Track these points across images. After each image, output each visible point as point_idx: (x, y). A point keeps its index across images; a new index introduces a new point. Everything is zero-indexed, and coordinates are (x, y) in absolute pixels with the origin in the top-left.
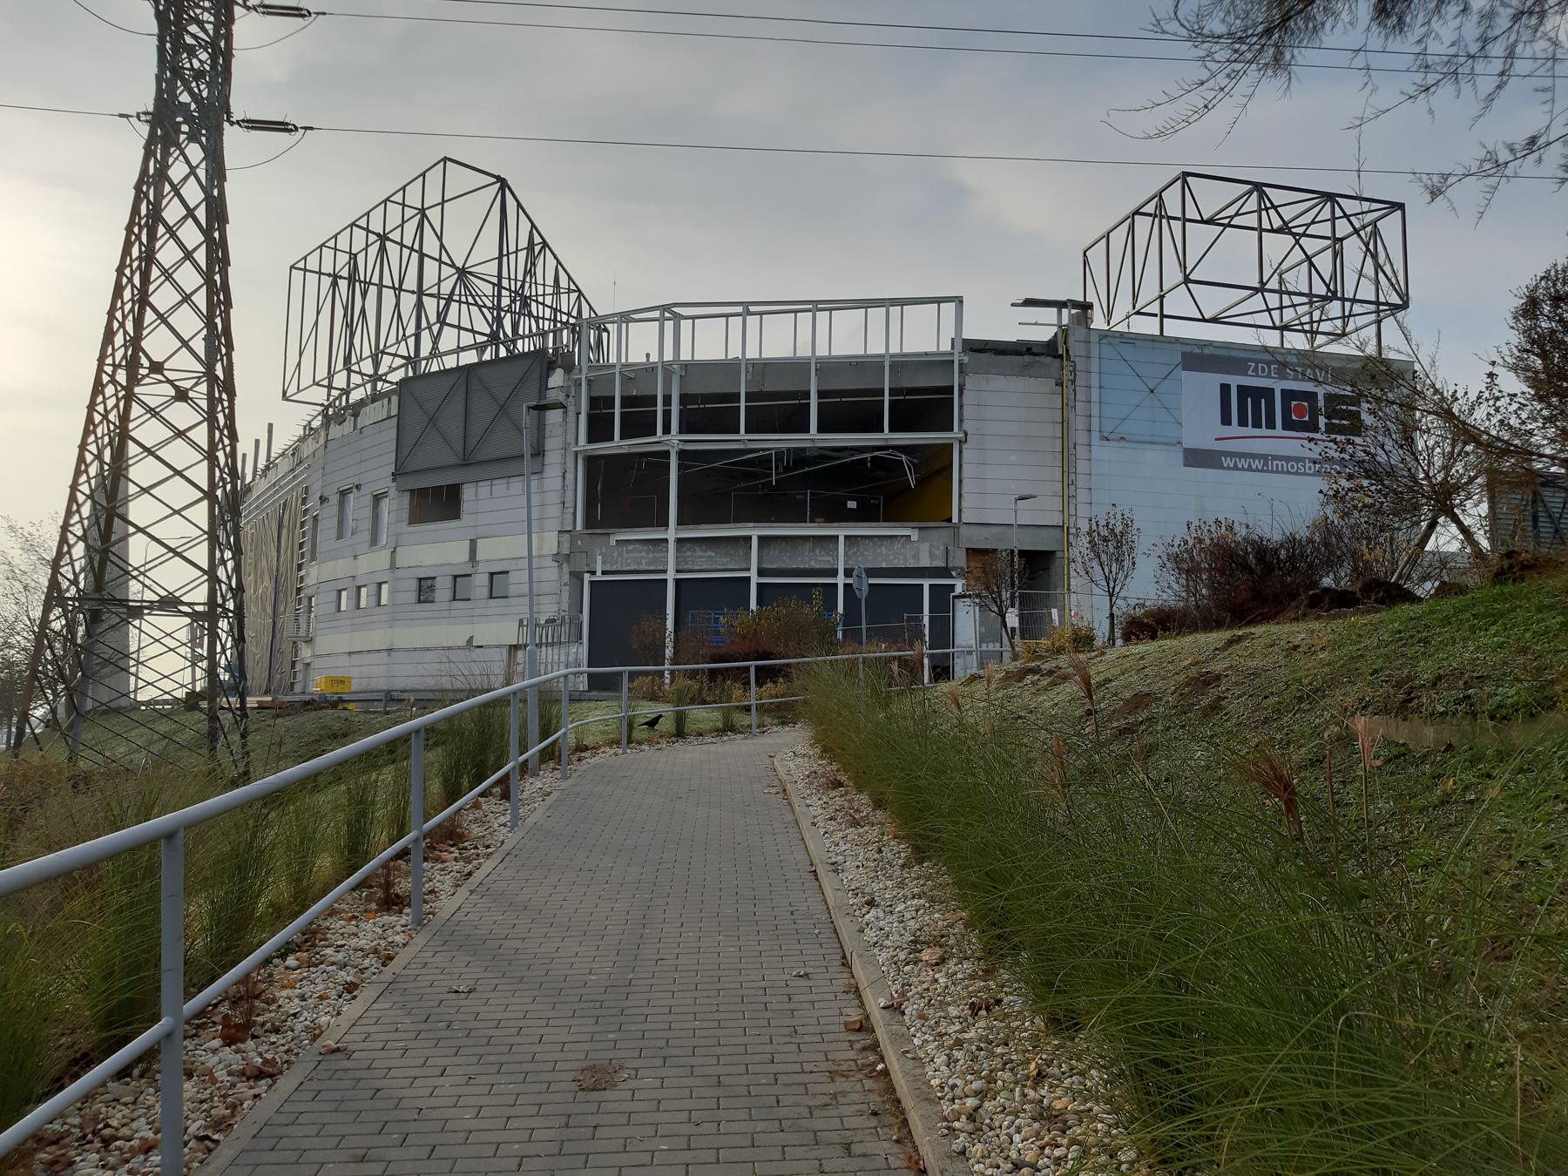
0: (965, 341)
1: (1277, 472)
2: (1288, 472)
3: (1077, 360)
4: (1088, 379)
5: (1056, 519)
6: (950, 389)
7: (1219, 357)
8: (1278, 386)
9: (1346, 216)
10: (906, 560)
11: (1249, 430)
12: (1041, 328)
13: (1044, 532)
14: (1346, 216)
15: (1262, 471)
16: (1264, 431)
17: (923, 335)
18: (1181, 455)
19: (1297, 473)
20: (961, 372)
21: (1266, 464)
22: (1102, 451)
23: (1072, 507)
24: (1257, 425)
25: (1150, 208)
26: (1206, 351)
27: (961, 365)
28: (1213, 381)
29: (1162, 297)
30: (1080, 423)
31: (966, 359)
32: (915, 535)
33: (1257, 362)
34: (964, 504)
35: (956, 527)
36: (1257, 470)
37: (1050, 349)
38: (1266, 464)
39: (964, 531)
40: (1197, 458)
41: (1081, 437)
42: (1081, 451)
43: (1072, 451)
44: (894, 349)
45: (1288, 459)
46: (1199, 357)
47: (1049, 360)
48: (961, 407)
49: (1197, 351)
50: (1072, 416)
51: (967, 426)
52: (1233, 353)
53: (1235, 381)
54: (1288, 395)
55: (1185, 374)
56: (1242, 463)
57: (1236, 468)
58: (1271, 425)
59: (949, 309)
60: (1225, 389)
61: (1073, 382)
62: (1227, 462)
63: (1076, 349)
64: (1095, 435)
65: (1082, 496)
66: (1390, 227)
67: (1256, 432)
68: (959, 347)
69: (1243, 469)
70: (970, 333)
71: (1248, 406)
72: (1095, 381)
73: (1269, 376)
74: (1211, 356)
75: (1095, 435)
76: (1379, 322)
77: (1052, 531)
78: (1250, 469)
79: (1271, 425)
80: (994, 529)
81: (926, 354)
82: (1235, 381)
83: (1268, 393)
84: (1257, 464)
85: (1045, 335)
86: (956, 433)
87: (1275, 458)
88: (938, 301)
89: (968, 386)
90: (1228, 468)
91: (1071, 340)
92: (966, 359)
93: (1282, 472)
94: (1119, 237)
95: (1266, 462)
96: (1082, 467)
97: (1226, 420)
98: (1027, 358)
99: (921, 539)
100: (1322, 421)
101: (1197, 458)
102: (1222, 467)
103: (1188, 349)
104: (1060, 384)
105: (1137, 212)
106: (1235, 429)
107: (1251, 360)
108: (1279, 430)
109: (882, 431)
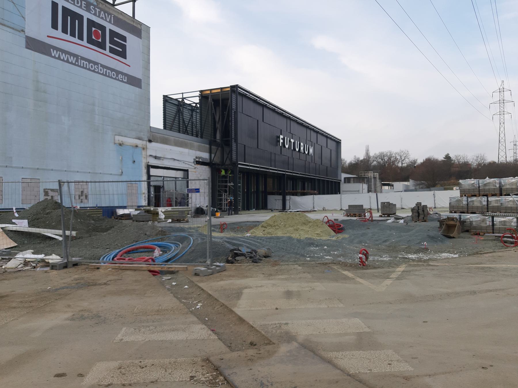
1: (83, 67)
2: (89, 69)
8: (86, 15)
11: (68, 37)
15: (75, 64)
16: (76, 40)
19: (94, 71)
24: (73, 35)
36: (71, 63)
40: (33, 44)
45: (90, 61)
54: (91, 23)
57: (59, 58)
58: (81, 38)
62: (54, 53)
67: (72, 39)
69: (63, 60)
73: (81, 7)
78: (67, 61)
79: (81, 38)
84: (71, 59)
87: (83, 58)
90: (54, 57)
93: (86, 68)
95: (77, 60)
97: (55, 26)
100: (108, 45)
101: (33, 44)
106: (59, 33)
108: (85, 42)
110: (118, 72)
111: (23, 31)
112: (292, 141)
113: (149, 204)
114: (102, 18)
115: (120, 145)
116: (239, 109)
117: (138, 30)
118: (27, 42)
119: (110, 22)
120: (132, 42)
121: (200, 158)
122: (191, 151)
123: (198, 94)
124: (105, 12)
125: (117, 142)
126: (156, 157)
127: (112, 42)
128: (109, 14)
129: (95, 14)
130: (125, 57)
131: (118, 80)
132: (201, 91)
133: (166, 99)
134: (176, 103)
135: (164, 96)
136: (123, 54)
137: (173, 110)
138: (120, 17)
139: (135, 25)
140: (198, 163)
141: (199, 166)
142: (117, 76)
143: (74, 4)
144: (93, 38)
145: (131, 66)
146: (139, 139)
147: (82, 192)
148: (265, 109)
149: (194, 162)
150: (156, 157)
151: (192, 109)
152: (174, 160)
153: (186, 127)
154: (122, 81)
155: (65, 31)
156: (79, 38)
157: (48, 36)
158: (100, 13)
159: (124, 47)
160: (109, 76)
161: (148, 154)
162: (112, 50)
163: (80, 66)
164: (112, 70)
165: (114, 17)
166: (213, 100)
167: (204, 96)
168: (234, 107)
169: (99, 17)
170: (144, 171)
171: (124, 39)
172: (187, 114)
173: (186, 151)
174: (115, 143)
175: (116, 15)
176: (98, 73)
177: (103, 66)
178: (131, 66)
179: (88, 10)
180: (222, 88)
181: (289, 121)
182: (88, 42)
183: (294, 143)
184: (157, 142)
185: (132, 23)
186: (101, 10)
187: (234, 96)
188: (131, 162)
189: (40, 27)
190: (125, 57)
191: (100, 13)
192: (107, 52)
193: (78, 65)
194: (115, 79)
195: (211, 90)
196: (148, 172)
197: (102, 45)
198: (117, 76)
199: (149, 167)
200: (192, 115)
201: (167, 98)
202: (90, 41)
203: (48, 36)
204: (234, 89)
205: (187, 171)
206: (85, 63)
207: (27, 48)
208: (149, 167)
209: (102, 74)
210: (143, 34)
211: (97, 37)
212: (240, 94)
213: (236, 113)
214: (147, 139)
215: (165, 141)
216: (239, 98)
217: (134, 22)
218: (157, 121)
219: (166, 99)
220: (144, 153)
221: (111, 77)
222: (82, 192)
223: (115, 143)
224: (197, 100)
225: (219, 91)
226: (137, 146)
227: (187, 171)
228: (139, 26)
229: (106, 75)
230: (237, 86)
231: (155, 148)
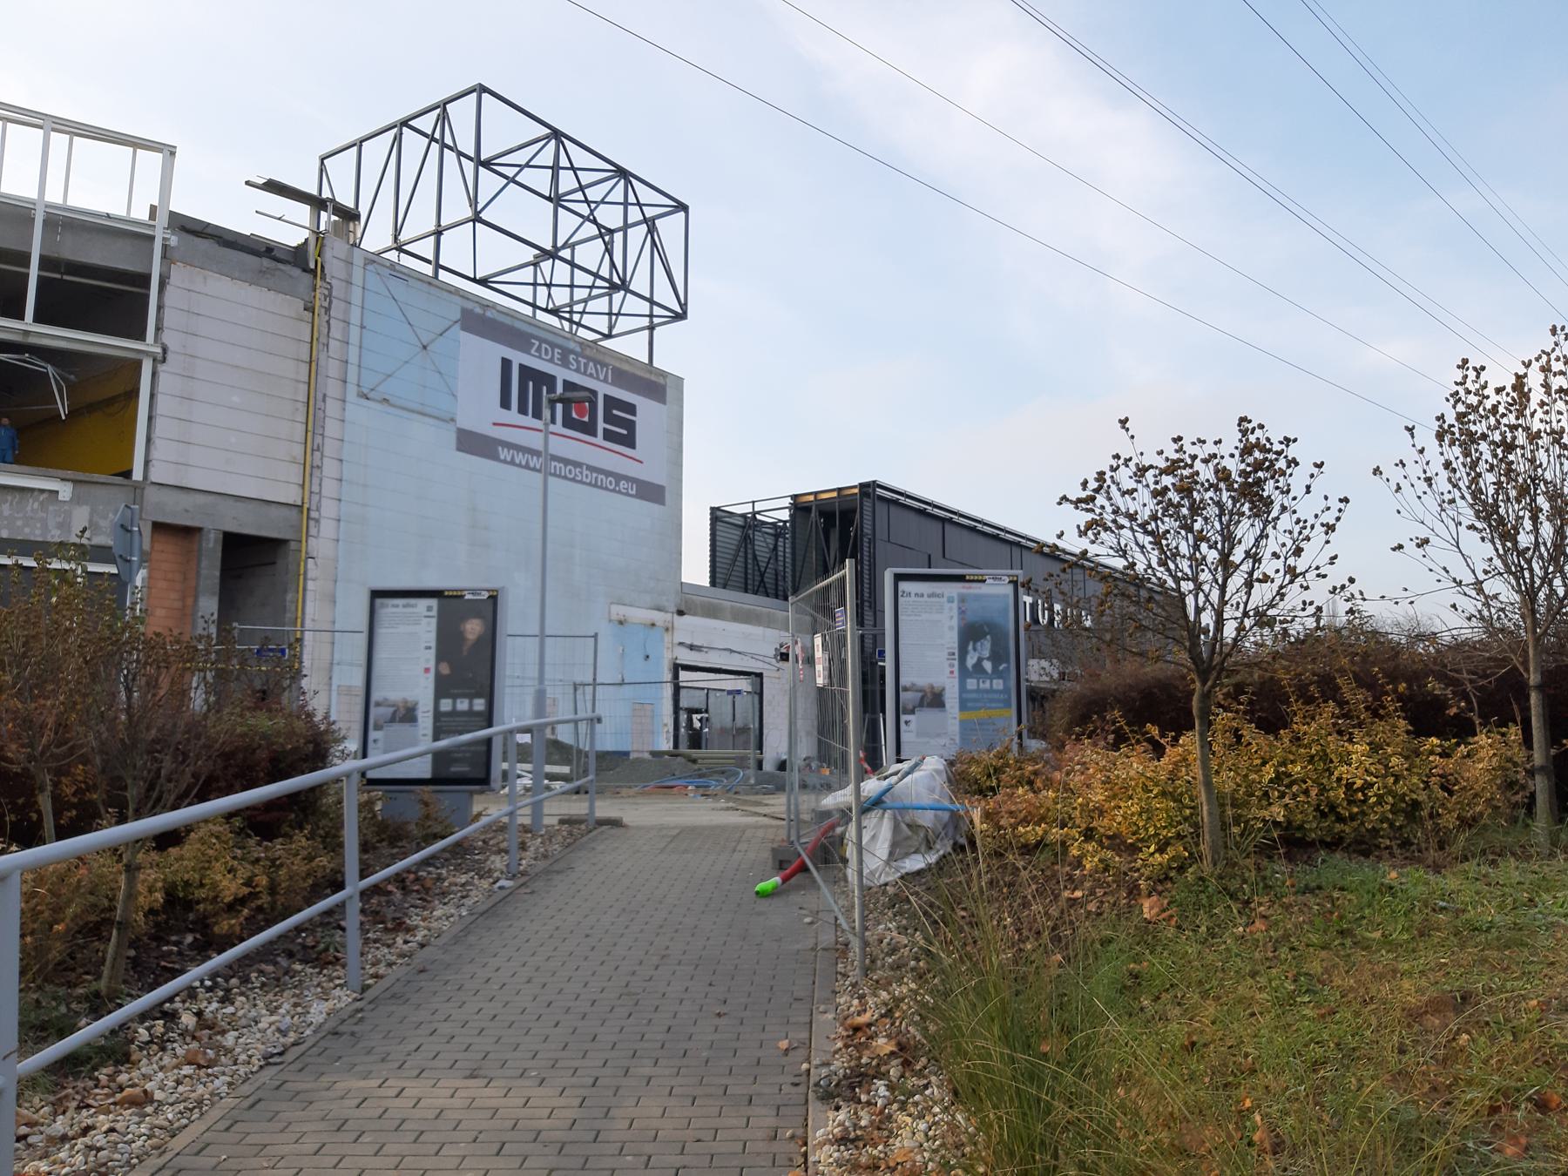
0: (173, 215)
2: (565, 477)
3: (334, 282)
4: (347, 312)
5: (291, 495)
6: (144, 280)
7: (502, 324)
8: (562, 374)
9: (638, 204)
10: (45, 528)
11: (529, 420)
12: (288, 226)
13: (274, 511)
14: (638, 204)
17: (103, 187)
18: (452, 438)
19: (573, 480)
20: (164, 257)
22: (358, 411)
23: (316, 481)
25: (427, 123)
26: (488, 314)
27: (165, 247)
28: (497, 351)
29: (438, 233)
30: (332, 368)
31: (174, 241)
32: (65, 491)
34: (155, 454)
35: (138, 488)
37: (297, 256)
39: (151, 494)
40: (473, 443)
41: (333, 389)
42: (332, 408)
43: (320, 404)
44: (54, 196)
45: (566, 462)
46: (482, 322)
47: (297, 272)
48: (160, 308)
49: (478, 310)
50: (323, 356)
51: (167, 337)
52: (518, 325)
53: (518, 358)
55: (466, 337)
56: (519, 458)
57: (512, 463)
59: (151, 162)
60: (506, 364)
61: (328, 310)
62: (504, 453)
63: (334, 268)
64: (352, 391)
65: (330, 468)
66: (670, 228)
68: (162, 220)
69: (520, 465)
70: (178, 206)
71: (528, 389)
72: (355, 317)
73: (551, 361)
74: (493, 321)
75: (352, 391)
76: (651, 328)
77: (285, 511)
80: (201, 499)
81: (108, 216)
82: (518, 358)
83: (550, 380)
85: (292, 237)
86: (149, 344)
88: (136, 143)
89: (172, 280)
90: (505, 462)
91: (328, 254)
92: (174, 241)
94: (376, 151)
96: (332, 428)
97: (505, 404)
98: (266, 262)
99: (76, 500)
100: (601, 425)
101: (473, 443)
102: (495, 457)
103: (469, 305)
104: (310, 308)
105: (405, 123)
106: (513, 416)
107: (536, 338)
109: (21, 317)
110: (619, 477)
111: (453, 420)
113: (676, 745)
114: (591, 375)
115: (621, 623)
116: (881, 534)
117: (657, 386)
119: (605, 381)
122: (769, 631)
123: (787, 502)
124: (596, 362)
126: (692, 647)
127: (609, 418)
128: (604, 365)
129: (577, 370)
130: (632, 445)
132: (795, 497)
133: (717, 516)
134: (740, 522)
135: (714, 510)
136: (629, 441)
137: (731, 537)
138: (626, 367)
139: (653, 378)
142: (617, 484)
145: (644, 462)
146: (659, 609)
148: (947, 527)
150: (692, 647)
151: (777, 530)
152: (732, 651)
153: (762, 575)
154: (627, 494)
155: (523, 410)
158: (586, 365)
159: (631, 426)
160: (601, 487)
161: (676, 641)
162: (609, 436)
164: (608, 474)
165: (615, 370)
166: (822, 514)
167: (800, 507)
168: (867, 529)
169: (585, 373)
170: (668, 676)
171: (631, 409)
172: (762, 545)
173: (756, 630)
175: (617, 365)
176: (581, 482)
177: (592, 469)
178: (644, 462)
179: (565, 363)
180: (839, 490)
181: (1016, 551)
182: (564, 425)
183: (1034, 606)
184: (695, 614)
185: (647, 376)
186: (589, 359)
187: (867, 504)
188: (642, 657)
189: (481, 408)
190: (632, 445)
191: (586, 365)
192: (599, 440)
194: (613, 490)
195: (816, 494)
196: (676, 676)
197: (590, 429)
198: (617, 484)
199: (677, 668)
200: (776, 546)
204: (868, 489)
205: (760, 675)
207: (459, 449)
208: (677, 668)
209: (590, 484)
210: (670, 393)
211: (578, 410)
212: (881, 498)
213: (873, 541)
215: (712, 612)
216: (881, 509)
218: (696, 568)
219: (718, 516)
220: (667, 638)
221: (606, 489)
224: (785, 515)
225: (835, 494)
227: (760, 675)
228: (661, 381)
229: (595, 486)
230: (875, 484)
231: (692, 627)
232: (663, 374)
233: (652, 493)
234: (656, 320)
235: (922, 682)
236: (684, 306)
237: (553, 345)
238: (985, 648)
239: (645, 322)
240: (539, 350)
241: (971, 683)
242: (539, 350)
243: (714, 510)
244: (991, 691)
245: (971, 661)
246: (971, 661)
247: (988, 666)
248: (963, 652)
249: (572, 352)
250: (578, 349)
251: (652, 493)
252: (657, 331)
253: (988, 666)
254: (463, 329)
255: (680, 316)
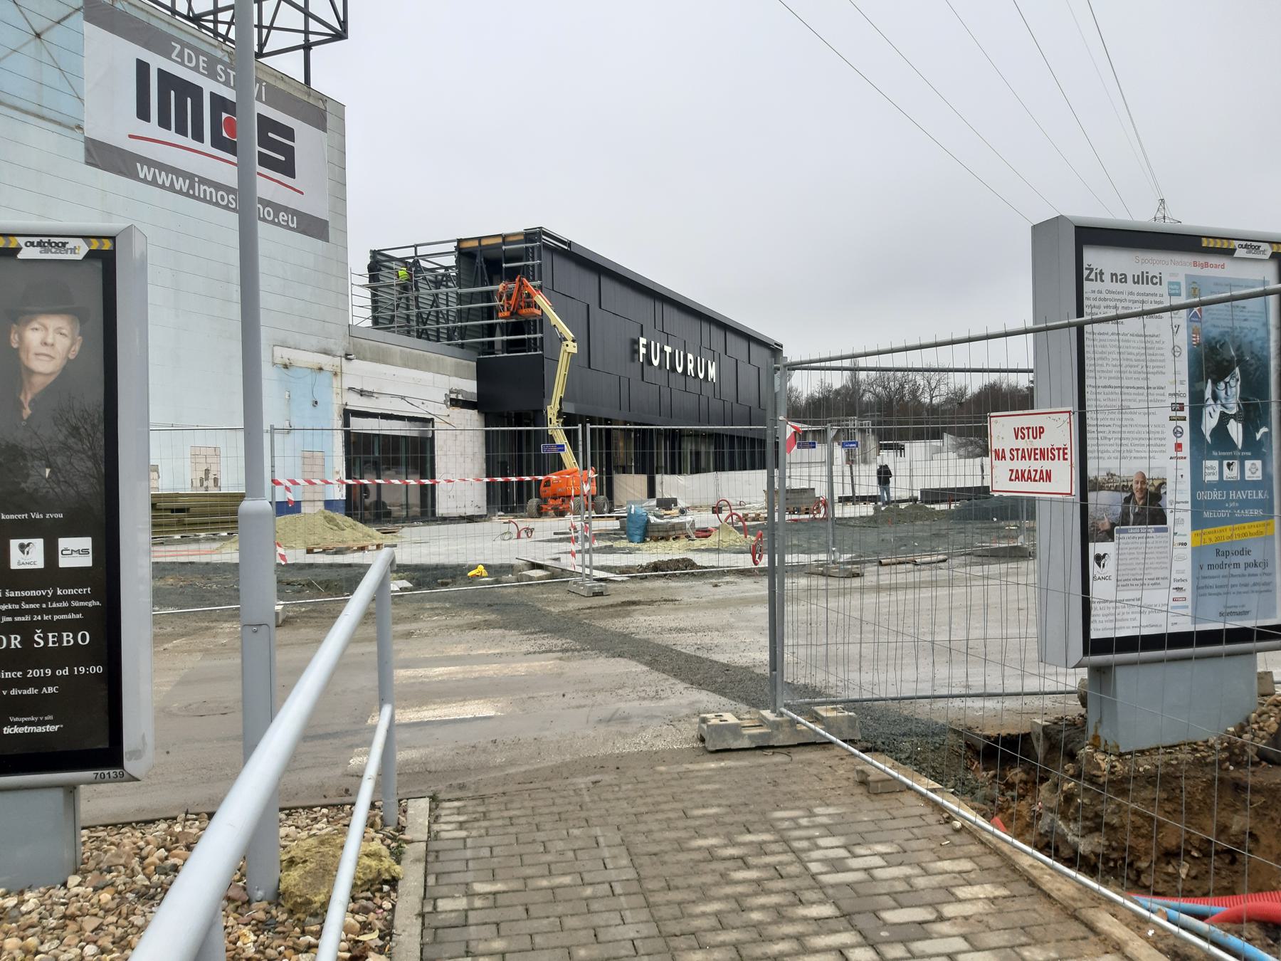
1: (204, 200)
2: (217, 204)
8: (209, 87)
11: (171, 135)
15: (187, 195)
16: (188, 141)
21: (192, 186)
24: (181, 130)
28: (130, 52)
33: (184, 45)
36: (180, 192)
38: (192, 186)
40: (103, 156)
53: (157, 62)
55: (89, 28)
56: (162, 178)
57: (154, 183)
58: (198, 136)
60: (142, 68)
62: (143, 172)
67: (179, 139)
69: (163, 187)
71: (170, 101)
73: (196, 69)
76: (307, 47)
78: (172, 188)
79: (198, 136)
82: (157, 62)
84: (180, 184)
87: (203, 181)
90: (144, 181)
93: (210, 202)
97: (143, 114)
101: (103, 156)
102: (135, 176)
106: (152, 128)
108: (207, 146)
111: (79, 127)
112: (668, 349)
115: (286, 367)
117: (320, 112)
118: (87, 150)
120: (306, 139)
121: (458, 392)
123: (451, 247)
125: (278, 360)
126: (362, 393)
127: (264, 141)
131: (279, 224)
132: (459, 241)
133: (378, 263)
135: (375, 254)
136: (288, 168)
138: (281, 86)
139: (311, 101)
140: (455, 403)
141: (457, 410)
142: (276, 215)
143: (182, 64)
144: (225, 134)
146: (326, 353)
147: (207, 471)
149: (445, 403)
150: (362, 393)
155: (164, 123)
156: (193, 138)
157: (131, 136)
159: (289, 152)
161: (346, 386)
163: (198, 198)
165: (268, 86)
166: (487, 261)
170: (339, 423)
171: (289, 133)
173: (427, 376)
174: (274, 364)
175: (271, 81)
179: (213, 75)
183: (672, 355)
184: (364, 359)
188: (309, 405)
193: (193, 197)
194: (272, 222)
195: (480, 239)
196: (346, 423)
198: (276, 215)
199: (348, 414)
201: (379, 257)
202: (218, 142)
203: (131, 136)
204: (532, 235)
206: (208, 190)
207: (87, 163)
208: (348, 414)
212: (546, 247)
214: (343, 354)
215: (380, 357)
217: (309, 95)
218: (360, 310)
222: (207, 471)
223: (274, 364)
224: (451, 261)
226: (321, 369)
231: (361, 372)
232: (323, 98)
233: (314, 227)
234: (313, 38)
235: (1129, 469)
236: (344, 23)
237: (198, 52)
238: (1232, 391)
239: (299, 39)
240: (181, 55)
241: (1211, 469)
242: (181, 55)
243: (375, 254)
244: (1242, 484)
245: (1210, 423)
246: (1210, 423)
247: (1235, 430)
248: (1197, 401)
249: (221, 61)
250: (226, 59)
251: (314, 227)
252: (315, 51)
253: (1235, 430)
254: (89, 18)
255: (340, 35)
